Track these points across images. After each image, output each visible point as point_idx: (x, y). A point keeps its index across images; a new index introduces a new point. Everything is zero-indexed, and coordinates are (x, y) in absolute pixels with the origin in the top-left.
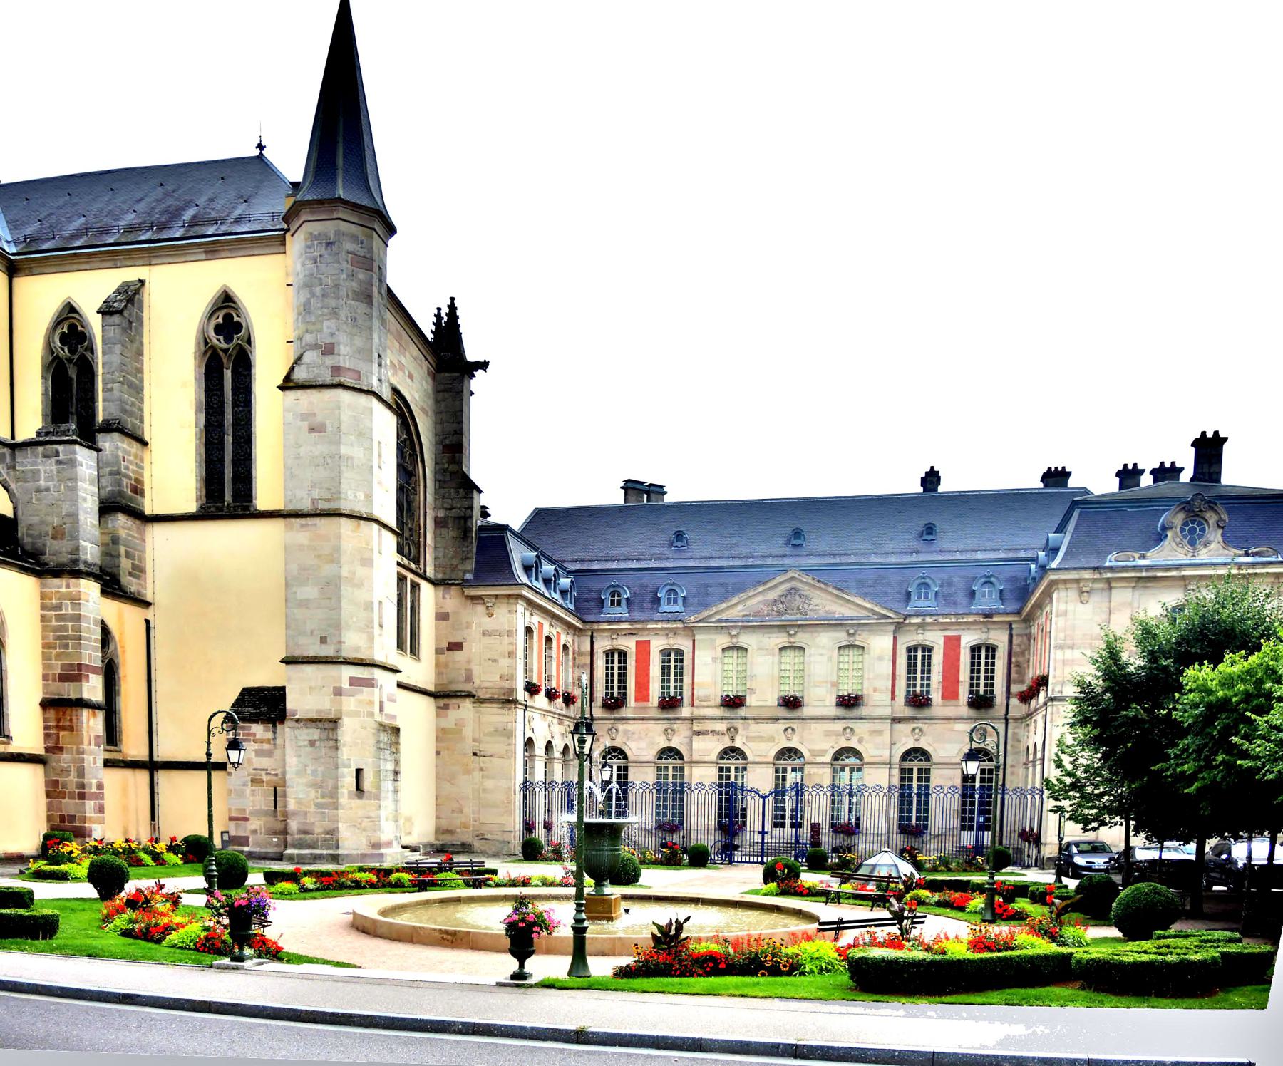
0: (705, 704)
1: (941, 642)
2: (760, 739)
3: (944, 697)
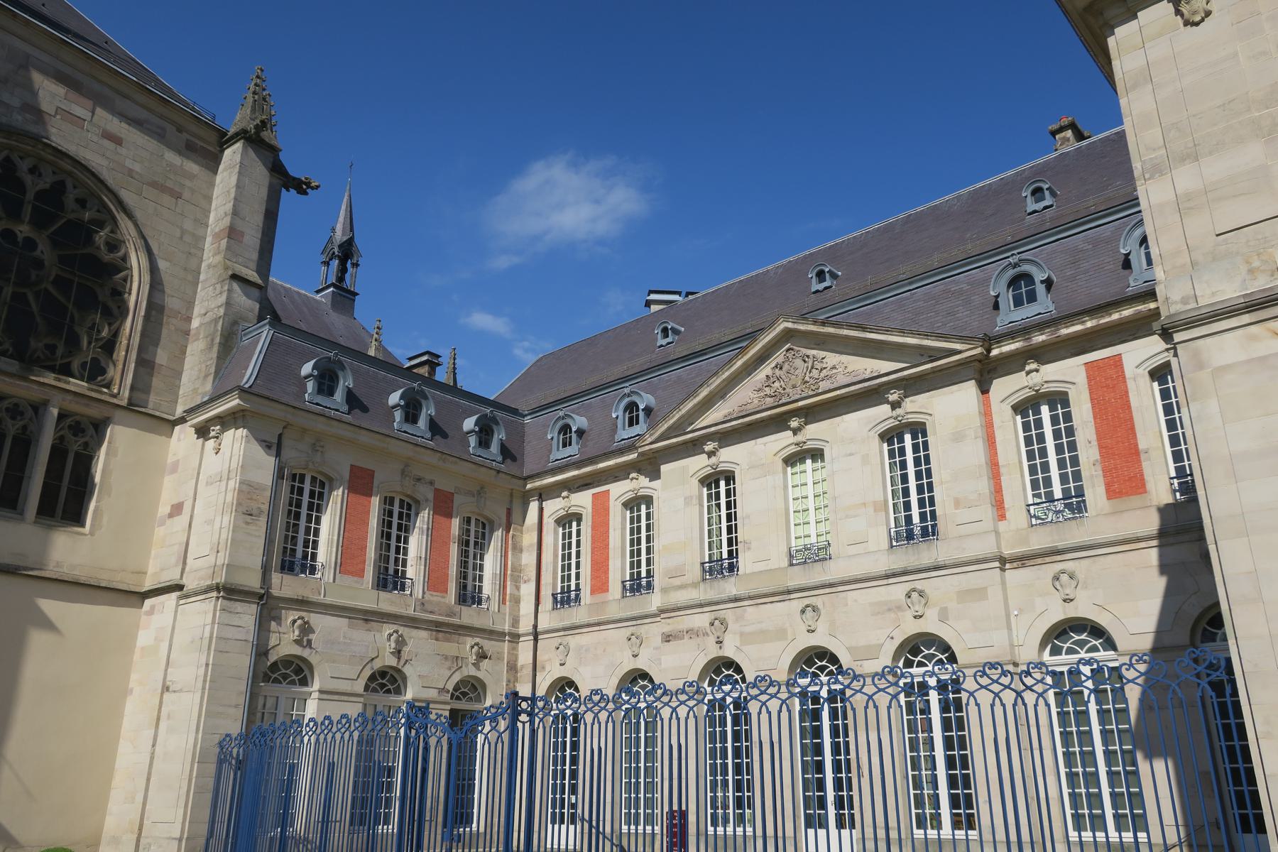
0: (677, 582)
1: (1081, 378)
2: (762, 636)
3: (1112, 493)
